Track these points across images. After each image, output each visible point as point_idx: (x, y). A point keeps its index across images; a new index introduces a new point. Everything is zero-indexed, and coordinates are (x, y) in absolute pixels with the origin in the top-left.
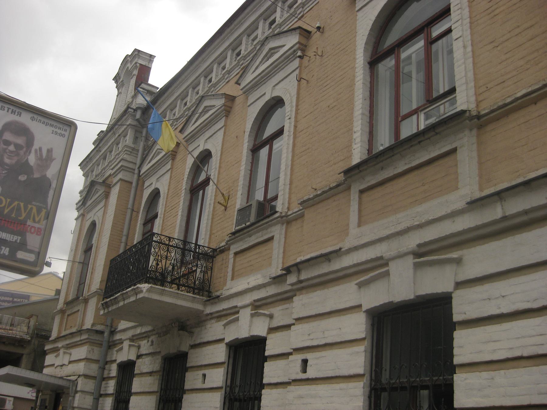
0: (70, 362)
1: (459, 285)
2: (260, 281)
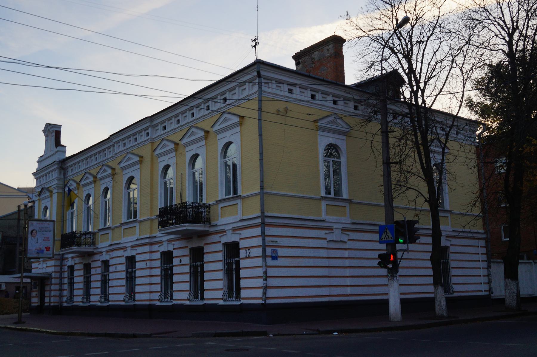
1: (137, 254)
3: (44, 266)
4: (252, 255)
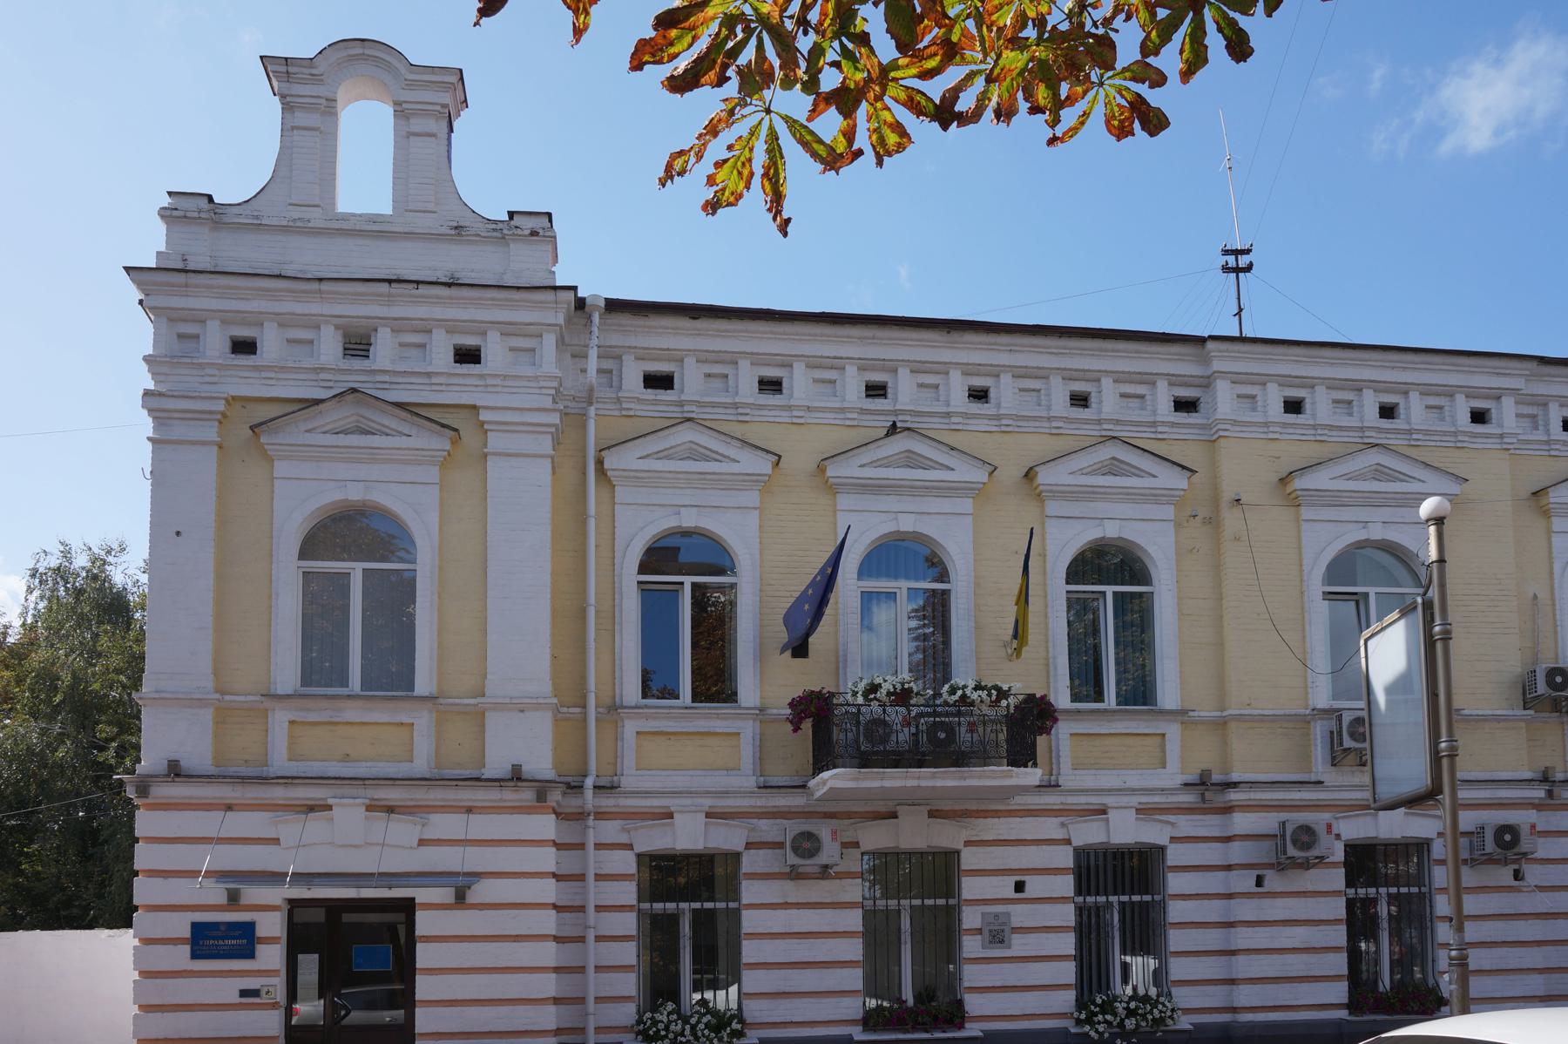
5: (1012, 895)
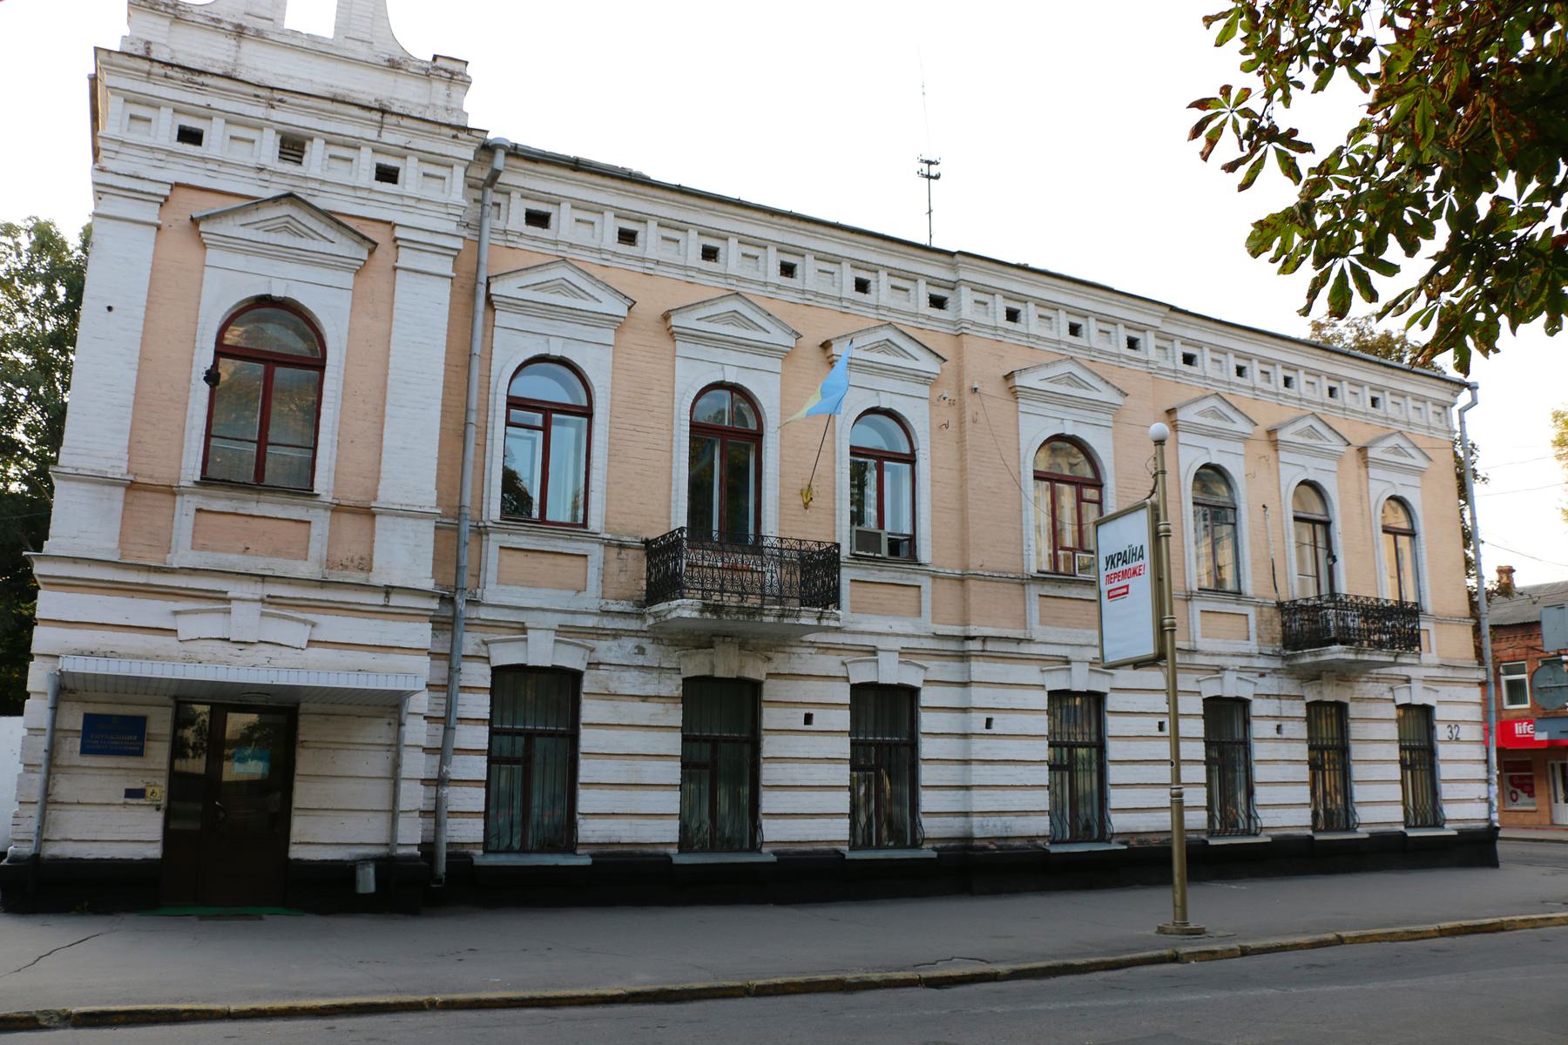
0: (311, 643)
2: (911, 630)
3: (291, 632)
4: (1462, 736)
5: (1274, 734)
